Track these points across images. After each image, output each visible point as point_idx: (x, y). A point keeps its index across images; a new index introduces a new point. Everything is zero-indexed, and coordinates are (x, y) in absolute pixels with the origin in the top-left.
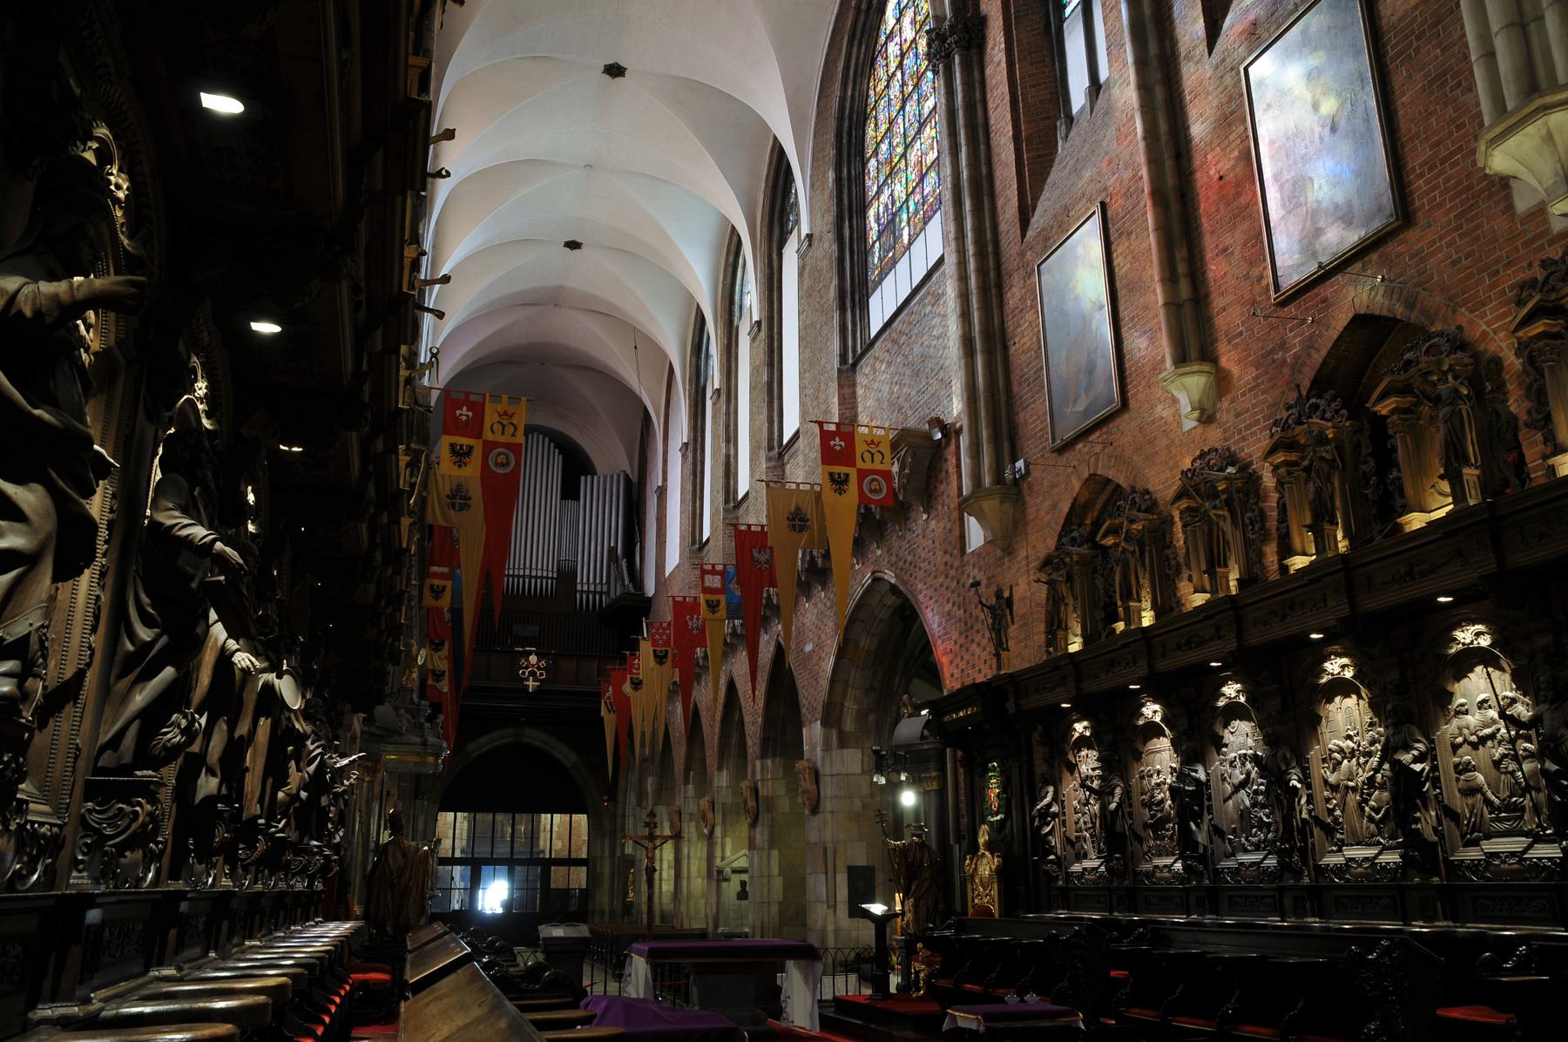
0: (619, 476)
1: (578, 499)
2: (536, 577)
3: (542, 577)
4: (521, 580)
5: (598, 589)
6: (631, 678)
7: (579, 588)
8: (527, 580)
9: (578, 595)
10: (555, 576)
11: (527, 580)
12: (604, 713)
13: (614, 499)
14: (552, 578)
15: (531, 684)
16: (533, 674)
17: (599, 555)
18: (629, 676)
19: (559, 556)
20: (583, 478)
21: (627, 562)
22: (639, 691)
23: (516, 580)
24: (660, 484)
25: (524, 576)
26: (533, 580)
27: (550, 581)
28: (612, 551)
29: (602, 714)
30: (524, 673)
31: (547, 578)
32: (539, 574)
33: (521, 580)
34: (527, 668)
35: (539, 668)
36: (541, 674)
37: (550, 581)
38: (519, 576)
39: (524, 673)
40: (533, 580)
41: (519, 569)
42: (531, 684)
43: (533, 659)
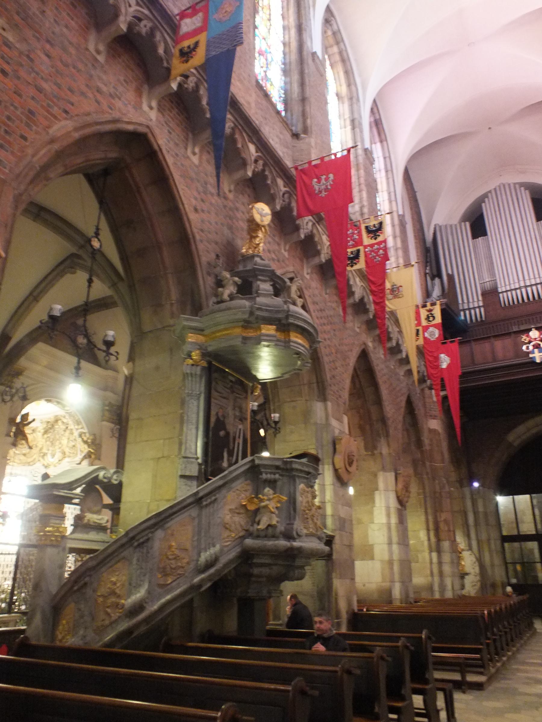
30: (528, 348)
34: (530, 342)
39: (528, 348)
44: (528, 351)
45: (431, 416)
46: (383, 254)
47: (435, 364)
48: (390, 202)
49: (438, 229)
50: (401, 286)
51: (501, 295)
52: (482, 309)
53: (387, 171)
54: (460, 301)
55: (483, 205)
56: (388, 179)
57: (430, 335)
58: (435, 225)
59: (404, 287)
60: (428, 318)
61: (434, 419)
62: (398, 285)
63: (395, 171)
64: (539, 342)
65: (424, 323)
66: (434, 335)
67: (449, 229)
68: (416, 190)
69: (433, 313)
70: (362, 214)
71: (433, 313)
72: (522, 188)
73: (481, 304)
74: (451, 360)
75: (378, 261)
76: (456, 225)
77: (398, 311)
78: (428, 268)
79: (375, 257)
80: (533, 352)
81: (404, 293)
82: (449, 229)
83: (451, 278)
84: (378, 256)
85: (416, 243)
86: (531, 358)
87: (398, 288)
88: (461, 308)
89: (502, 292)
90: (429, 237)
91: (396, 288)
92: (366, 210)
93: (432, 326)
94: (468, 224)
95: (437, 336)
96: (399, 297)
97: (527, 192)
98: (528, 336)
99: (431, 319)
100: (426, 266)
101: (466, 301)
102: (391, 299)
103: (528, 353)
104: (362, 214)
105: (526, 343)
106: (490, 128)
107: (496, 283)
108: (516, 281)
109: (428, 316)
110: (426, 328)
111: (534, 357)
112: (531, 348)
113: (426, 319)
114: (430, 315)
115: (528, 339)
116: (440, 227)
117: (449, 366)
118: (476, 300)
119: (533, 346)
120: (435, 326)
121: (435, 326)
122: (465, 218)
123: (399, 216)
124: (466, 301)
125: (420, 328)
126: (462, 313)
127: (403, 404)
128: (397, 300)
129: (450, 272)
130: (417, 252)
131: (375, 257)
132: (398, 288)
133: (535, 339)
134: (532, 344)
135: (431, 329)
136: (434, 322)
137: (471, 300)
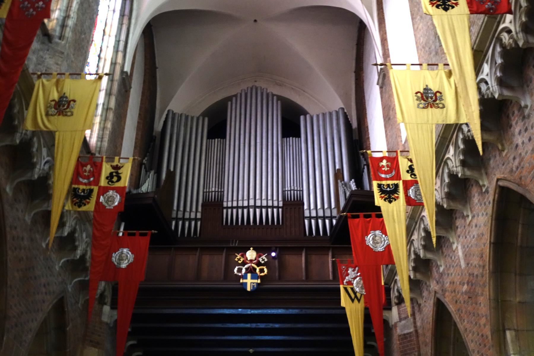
0: (337, 113)
1: (299, 136)
2: (261, 207)
3: (267, 207)
4: (245, 211)
5: (328, 214)
6: (379, 186)
7: (307, 214)
8: (251, 210)
9: (306, 222)
10: (281, 204)
11: (251, 210)
12: (345, 301)
13: (335, 132)
14: (278, 207)
15: (250, 282)
16: (251, 270)
17: (325, 182)
18: (375, 183)
19: (284, 186)
20: (302, 118)
21: (355, 182)
22: (394, 203)
23: (240, 211)
24: (380, 61)
25: (248, 207)
26: (258, 211)
27: (275, 210)
28: (339, 175)
29: (343, 304)
30: (240, 270)
31: (273, 207)
32: (264, 204)
33: (245, 211)
34: (244, 264)
35: (259, 264)
36: (262, 271)
37: (275, 210)
38: (243, 208)
39: (240, 270)
40: (258, 211)
41: (243, 200)
42: (250, 282)
43: (251, 254)
44: (240, 274)
45: (91, 341)
46: (42, 8)
47: (103, 243)
48: (116, 51)
49: (170, 115)
50: (74, 101)
51: (225, 211)
52: (199, 223)
53: (122, 15)
54: (175, 208)
55: (229, 103)
56: (121, 24)
57: (107, 202)
58: (169, 111)
59: (77, 103)
60: (110, 178)
61: (95, 347)
62: (71, 98)
63: (133, 21)
64: (255, 266)
65: (103, 182)
66: (114, 203)
67: (183, 118)
68: (157, 65)
69: (120, 171)
70: (63, 26)
71: (120, 171)
72: (275, 98)
73: (199, 216)
74: (135, 258)
75: (32, 15)
76: (192, 118)
77: (57, 133)
78: (146, 158)
79: (28, 9)
80: (245, 277)
81: (75, 111)
82: (183, 118)
83: (171, 175)
84: (33, 6)
85: (138, 122)
86: (242, 283)
87: (69, 102)
88: (174, 215)
89: (227, 208)
90: (158, 126)
91: (65, 101)
92: (70, 23)
93: (113, 189)
94: (206, 120)
95: (116, 204)
96: (66, 115)
97: (279, 102)
98: (244, 255)
99: (115, 179)
100: (145, 156)
101: (182, 208)
102: (52, 115)
103: (240, 277)
104: (63, 26)
105: (239, 265)
106: (255, 21)
107: (222, 196)
108: (246, 197)
109: (111, 174)
110: (103, 191)
111: (246, 283)
112: (244, 271)
113: (107, 178)
114: (114, 174)
115: (242, 260)
116: (174, 114)
117: (130, 266)
118: (194, 209)
119: (247, 269)
120: (119, 190)
121: (119, 190)
122: (204, 114)
123: (122, 72)
124: (182, 208)
125: (96, 189)
126: (174, 223)
127: (47, 307)
128: (61, 117)
129: (172, 169)
130: (137, 134)
131: (28, 9)
132: (69, 102)
133: (251, 261)
134: (246, 266)
135: (111, 193)
136: (117, 185)
137: (188, 209)
